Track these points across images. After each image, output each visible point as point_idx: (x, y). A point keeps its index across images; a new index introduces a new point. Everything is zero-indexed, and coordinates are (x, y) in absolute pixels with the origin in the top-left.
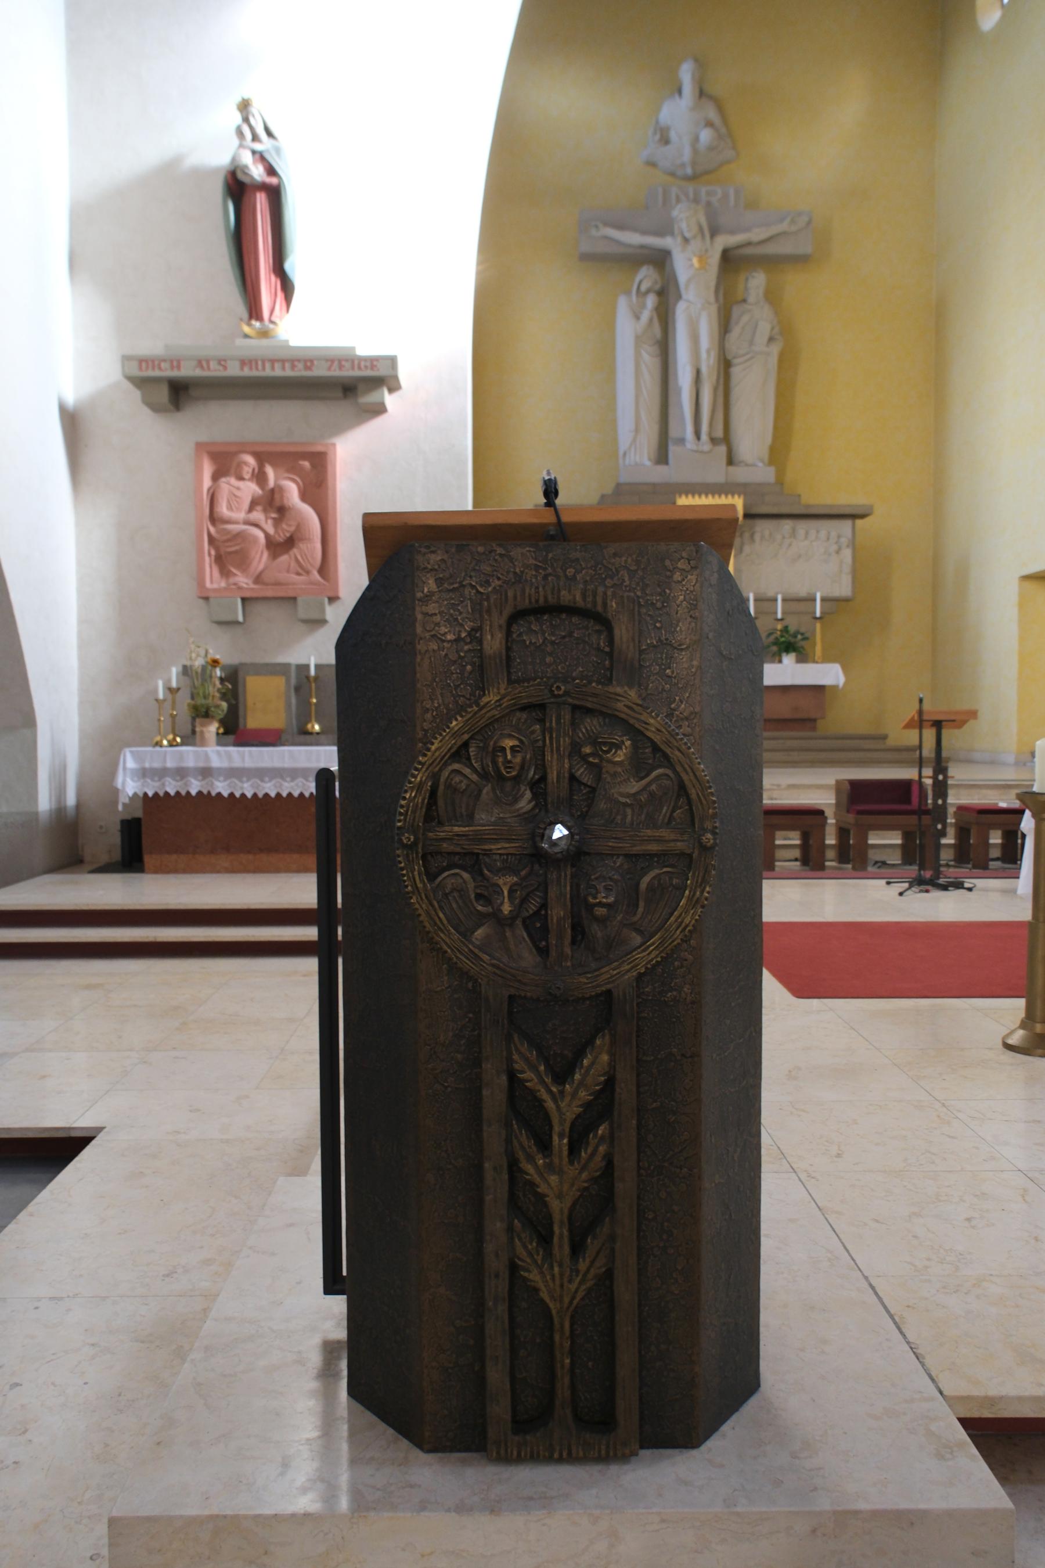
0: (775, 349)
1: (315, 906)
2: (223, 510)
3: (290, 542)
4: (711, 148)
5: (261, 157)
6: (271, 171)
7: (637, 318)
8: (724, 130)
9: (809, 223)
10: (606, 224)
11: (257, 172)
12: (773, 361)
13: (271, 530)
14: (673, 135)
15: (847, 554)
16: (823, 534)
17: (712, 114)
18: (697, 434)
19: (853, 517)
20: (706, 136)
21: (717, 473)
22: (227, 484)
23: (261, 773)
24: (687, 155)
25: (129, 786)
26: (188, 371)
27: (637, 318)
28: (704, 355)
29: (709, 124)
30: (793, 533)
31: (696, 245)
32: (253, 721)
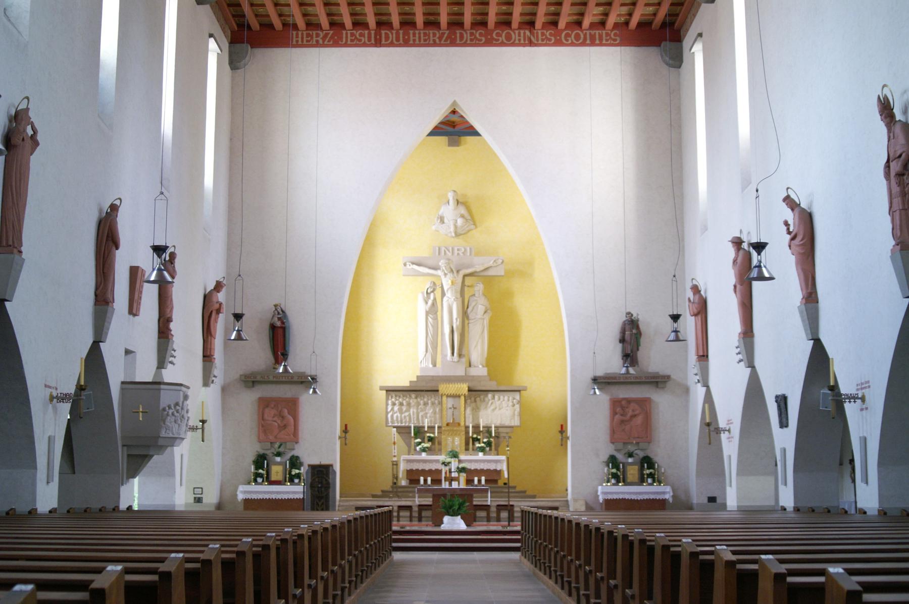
0: (487, 317)
1: (301, 496)
2: (266, 416)
3: (285, 426)
4: (462, 227)
5: (279, 319)
6: (283, 323)
7: (427, 303)
8: (469, 218)
9: (503, 262)
10: (413, 263)
11: (278, 324)
12: (486, 322)
13: (279, 422)
14: (446, 220)
15: (517, 406)
16: (506, 398)
17: (462, 210)
18: (453, 354)
19: (519, 391)
20: (460, 221)
21: (460, 371)
22: (267, 410)
23: (278, 493)
24: (452, 229)
25: (241, 497)
26: (259, 378)
27: (427, 303)
28: (454, 321)
29: (462, 216)
30: (494, 398)
31: (450, 275)
32: (274, 477)
